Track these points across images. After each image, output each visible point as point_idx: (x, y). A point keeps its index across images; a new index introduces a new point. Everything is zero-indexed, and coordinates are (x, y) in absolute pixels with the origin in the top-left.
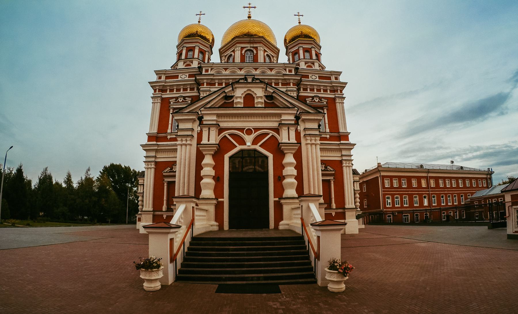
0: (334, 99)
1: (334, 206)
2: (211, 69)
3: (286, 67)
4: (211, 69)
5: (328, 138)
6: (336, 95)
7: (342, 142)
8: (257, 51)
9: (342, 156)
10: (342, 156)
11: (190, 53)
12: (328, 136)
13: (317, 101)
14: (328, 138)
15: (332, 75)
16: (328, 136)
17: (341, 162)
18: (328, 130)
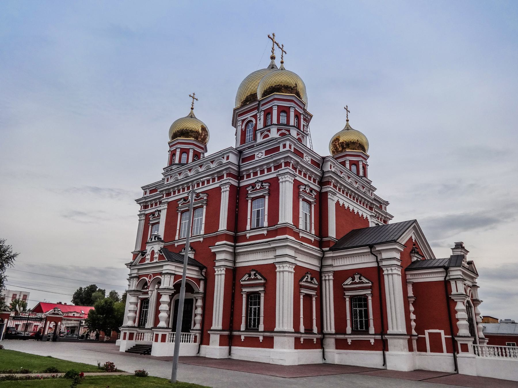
0: (276, 179)
1: (302, 329)
2: (171, 177)
3: (223, 154)
4: (171, 177)
5: (265, 235)
6: (280, 172)
7: (278, 237)
9: (277, 257)
10: (277, 257)
11: (184, 156)
12: (265, 232)
13: (258, 188)
14: (265, 235)
15: (279, 143)
16: (265, 232)
17: (273, 266)
18: (266, 224)
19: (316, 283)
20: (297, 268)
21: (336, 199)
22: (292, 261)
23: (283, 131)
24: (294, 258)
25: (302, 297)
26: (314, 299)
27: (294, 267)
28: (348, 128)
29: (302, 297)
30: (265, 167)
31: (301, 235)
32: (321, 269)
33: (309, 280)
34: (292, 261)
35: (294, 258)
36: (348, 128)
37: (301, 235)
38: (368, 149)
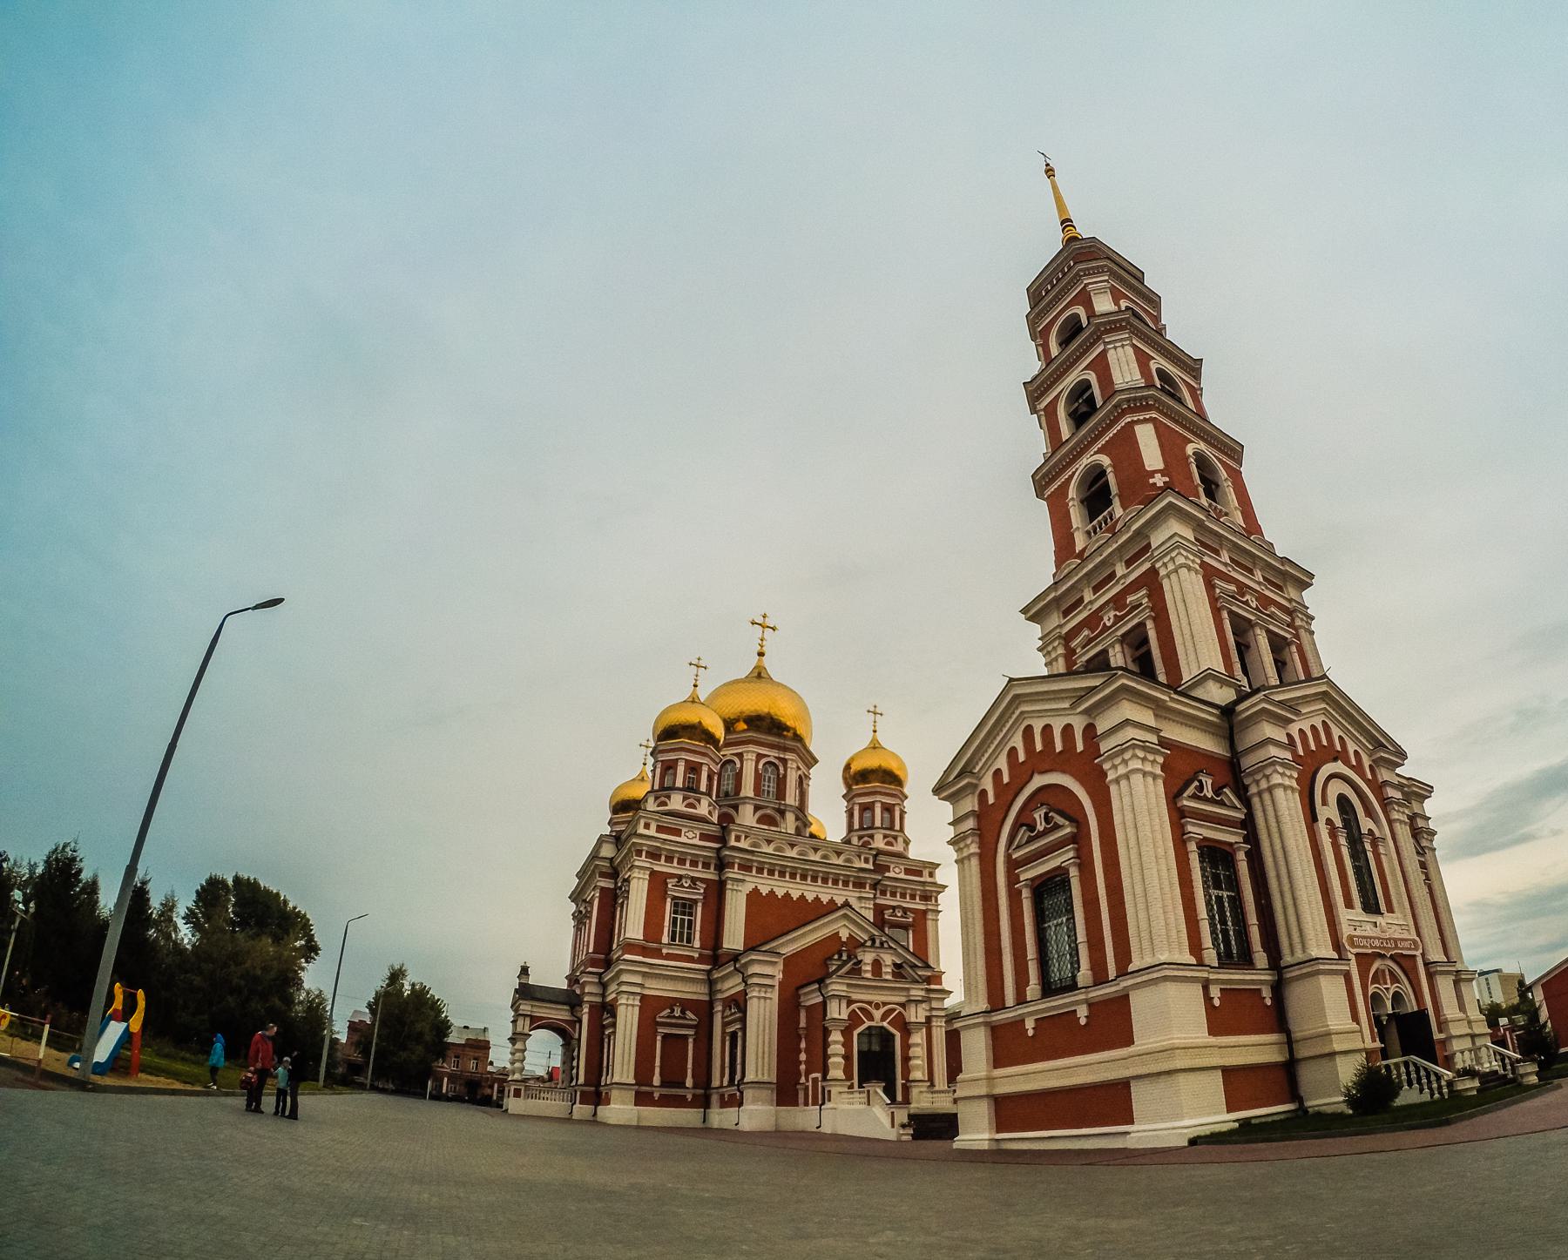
8: (785, 770)
19: (693, 1017)
20: (644, 998)
21: (749, 887)
22: (638, 990)
23: (691, 800)
24: (641, 986)
25: (659, 1038)
26: (691, 1040)
27: (639, 998)
28: (875, 746)
29: (659, 1038)
30: (677, 855)
31: (665, 951)
32: (711, 998)
33: (677, 1013)
34: (638, 990)
35: (641, 986)
36: (875, 746)
37: (665, 951)
38: (906, 776)
